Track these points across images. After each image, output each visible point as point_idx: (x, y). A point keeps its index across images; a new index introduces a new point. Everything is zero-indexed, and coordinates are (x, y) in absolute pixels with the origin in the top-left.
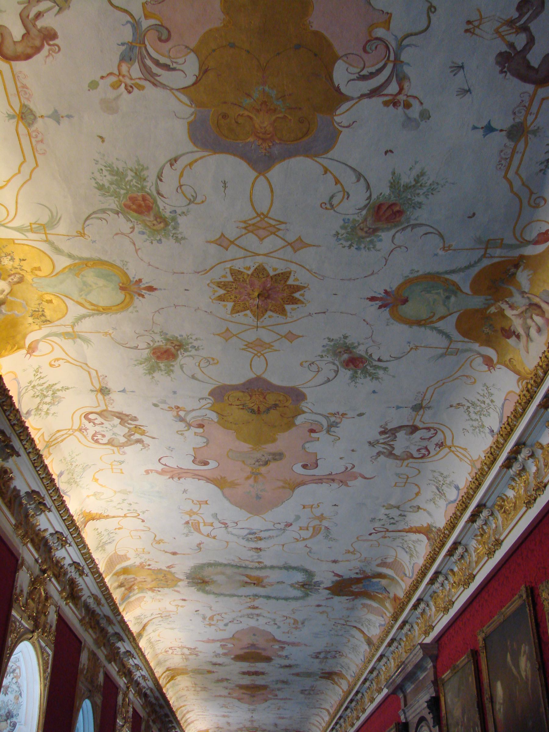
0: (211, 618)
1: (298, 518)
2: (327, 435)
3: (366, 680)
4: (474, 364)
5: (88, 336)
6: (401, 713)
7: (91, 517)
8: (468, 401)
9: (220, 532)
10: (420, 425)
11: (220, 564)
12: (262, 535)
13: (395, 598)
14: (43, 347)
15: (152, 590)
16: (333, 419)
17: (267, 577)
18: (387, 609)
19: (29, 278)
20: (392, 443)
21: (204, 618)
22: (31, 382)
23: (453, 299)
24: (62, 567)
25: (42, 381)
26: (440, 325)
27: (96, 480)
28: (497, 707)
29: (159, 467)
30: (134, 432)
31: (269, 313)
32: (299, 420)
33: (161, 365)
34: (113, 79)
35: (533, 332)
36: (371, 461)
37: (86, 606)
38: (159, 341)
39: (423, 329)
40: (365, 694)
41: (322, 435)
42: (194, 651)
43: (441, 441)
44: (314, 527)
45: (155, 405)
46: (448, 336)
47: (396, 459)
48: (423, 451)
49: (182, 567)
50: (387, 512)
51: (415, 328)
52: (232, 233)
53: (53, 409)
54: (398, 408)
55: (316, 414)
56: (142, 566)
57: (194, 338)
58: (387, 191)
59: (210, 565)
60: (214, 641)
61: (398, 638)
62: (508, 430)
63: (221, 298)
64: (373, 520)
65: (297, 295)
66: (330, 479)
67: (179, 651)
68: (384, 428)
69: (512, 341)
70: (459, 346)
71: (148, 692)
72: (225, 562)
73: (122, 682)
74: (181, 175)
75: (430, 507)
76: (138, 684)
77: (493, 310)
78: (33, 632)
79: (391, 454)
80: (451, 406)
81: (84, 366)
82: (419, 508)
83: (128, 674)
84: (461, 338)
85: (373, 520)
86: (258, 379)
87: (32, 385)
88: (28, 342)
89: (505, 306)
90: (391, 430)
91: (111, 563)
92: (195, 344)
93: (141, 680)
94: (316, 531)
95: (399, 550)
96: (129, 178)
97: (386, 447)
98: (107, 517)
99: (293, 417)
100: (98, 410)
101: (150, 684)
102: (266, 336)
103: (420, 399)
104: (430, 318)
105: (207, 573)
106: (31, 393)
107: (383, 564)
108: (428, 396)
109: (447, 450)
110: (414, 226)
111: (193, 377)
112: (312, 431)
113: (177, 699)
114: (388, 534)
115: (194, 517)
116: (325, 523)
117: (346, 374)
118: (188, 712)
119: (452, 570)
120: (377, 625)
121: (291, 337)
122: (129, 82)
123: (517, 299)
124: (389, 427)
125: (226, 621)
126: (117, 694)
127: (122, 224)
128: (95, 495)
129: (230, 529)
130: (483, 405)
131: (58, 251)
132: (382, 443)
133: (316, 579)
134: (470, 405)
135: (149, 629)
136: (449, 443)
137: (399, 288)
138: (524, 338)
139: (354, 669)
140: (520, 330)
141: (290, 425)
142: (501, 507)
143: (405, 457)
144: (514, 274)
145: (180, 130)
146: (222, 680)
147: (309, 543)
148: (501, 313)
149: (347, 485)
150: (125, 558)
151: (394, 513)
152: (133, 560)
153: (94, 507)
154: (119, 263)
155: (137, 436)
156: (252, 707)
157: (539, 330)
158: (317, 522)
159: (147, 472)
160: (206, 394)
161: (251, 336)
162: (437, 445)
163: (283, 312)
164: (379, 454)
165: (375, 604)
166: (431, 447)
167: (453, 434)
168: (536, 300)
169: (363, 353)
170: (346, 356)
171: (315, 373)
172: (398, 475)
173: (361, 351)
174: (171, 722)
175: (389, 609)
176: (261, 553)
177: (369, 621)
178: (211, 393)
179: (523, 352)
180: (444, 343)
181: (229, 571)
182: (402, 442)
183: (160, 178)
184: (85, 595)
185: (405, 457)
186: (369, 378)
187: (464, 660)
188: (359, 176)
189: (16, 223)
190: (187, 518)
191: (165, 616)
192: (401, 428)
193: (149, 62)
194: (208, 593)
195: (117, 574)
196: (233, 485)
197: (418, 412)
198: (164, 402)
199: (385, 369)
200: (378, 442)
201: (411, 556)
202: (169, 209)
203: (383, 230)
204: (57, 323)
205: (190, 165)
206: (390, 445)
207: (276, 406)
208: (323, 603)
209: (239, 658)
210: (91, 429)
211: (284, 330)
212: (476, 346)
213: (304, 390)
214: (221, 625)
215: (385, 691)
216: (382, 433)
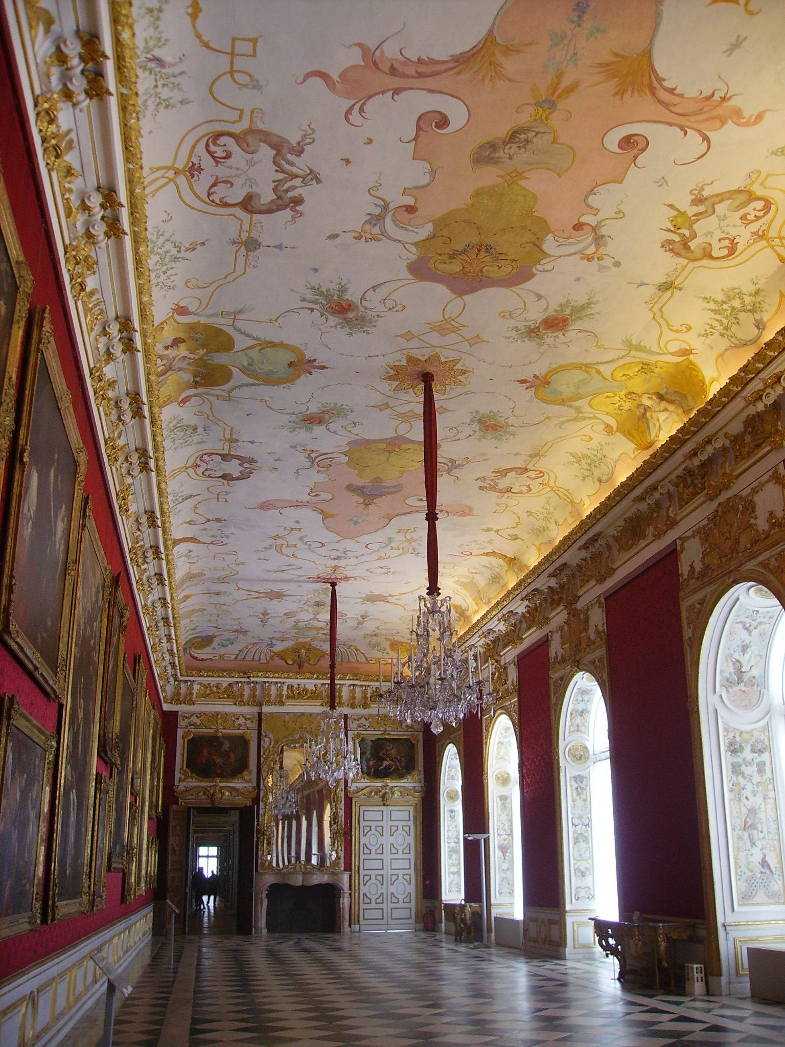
2: (389, 200)
4: (197, 303)
8: (183, 258)
10: (238, 211)
14: (674, 347)
16: (376, 230)
20: (281, 176)
22: (722, 335)
23: (246, 364)
25: (715, 323)
31: (423, 359)
32: (426, 231)
36: (313, 130)
39: (267, 339)
43: (196, 178)
45: (617, 264)
47: (266, 133)
51: (277, 341)
54: (280, 247)
55: (399, 241)
57: (511, 339)
63: (463, 372)
65: (393, 373)
68: (298, 212)
70: (223, 321)
80: (203, 244)
84: (224, 328)
86: (461, 294)
87: (725, 331)
89: (192, 356)
90: (285, 207)
97: (288, 167)
99: (434, 237)
102: (435, 339)
103: (250, 258)
104: (263, 349)
106: (734, 328)
109: (180, 165)
112: (411, 209)
117: (353, 295)
121: (409, 336)
123: (184, 365)
124: (287, 214)
130: (164, 269)
132: (297, 176)
134: (180, 255)
136: (182, 180)
137: (299, 376)
141: (441, 224)
143: (250, 139)
144: (195, 376)
161: (452, 338)
162: (200, 170)
166: (207, 162)
167: (181, 197)
170: (351, 315)
171: (391, 297)
173: (333, 320)
180: (239, 324)
185: (250, 139)
186: (323, 289)
197: (248, 238)
199: (304, 300)
200: (305, 183)
204: (638, 360)
206: (283, 172)
207: (452, 256)
211: (414, 343)
212: (203, 320)
213: (409, 276)
216: (298, 201)
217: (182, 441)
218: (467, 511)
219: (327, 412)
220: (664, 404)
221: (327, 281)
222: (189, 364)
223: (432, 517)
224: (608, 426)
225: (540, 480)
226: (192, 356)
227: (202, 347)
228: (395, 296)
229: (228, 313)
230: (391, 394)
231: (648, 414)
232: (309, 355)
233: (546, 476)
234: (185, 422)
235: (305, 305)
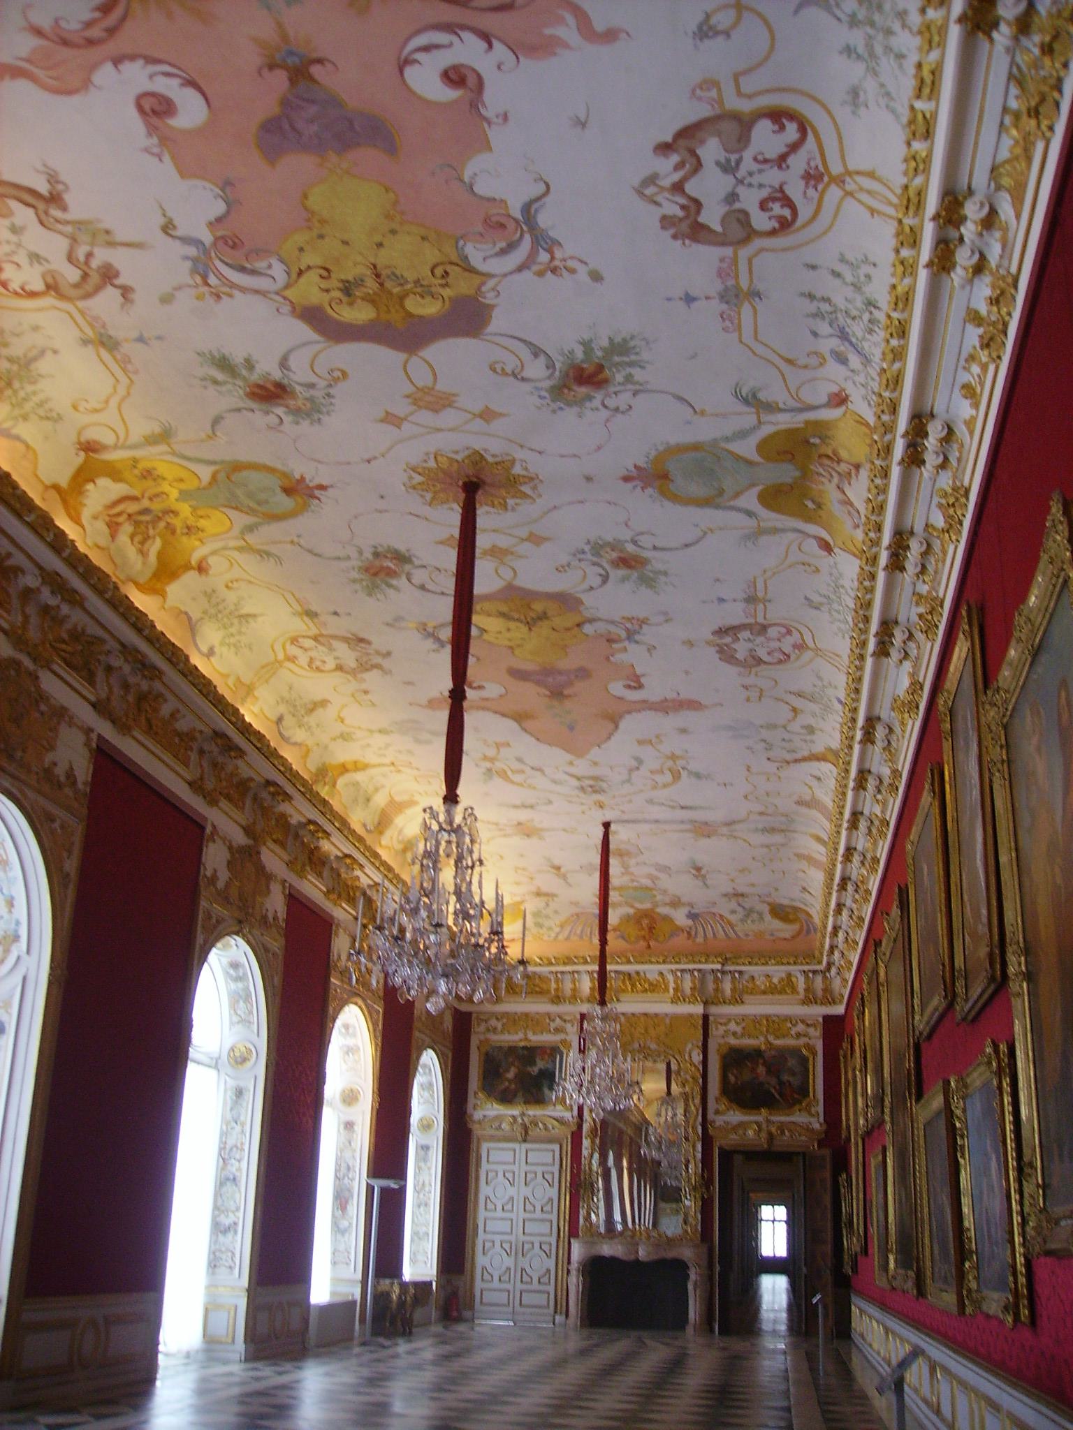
156: (582, 767)
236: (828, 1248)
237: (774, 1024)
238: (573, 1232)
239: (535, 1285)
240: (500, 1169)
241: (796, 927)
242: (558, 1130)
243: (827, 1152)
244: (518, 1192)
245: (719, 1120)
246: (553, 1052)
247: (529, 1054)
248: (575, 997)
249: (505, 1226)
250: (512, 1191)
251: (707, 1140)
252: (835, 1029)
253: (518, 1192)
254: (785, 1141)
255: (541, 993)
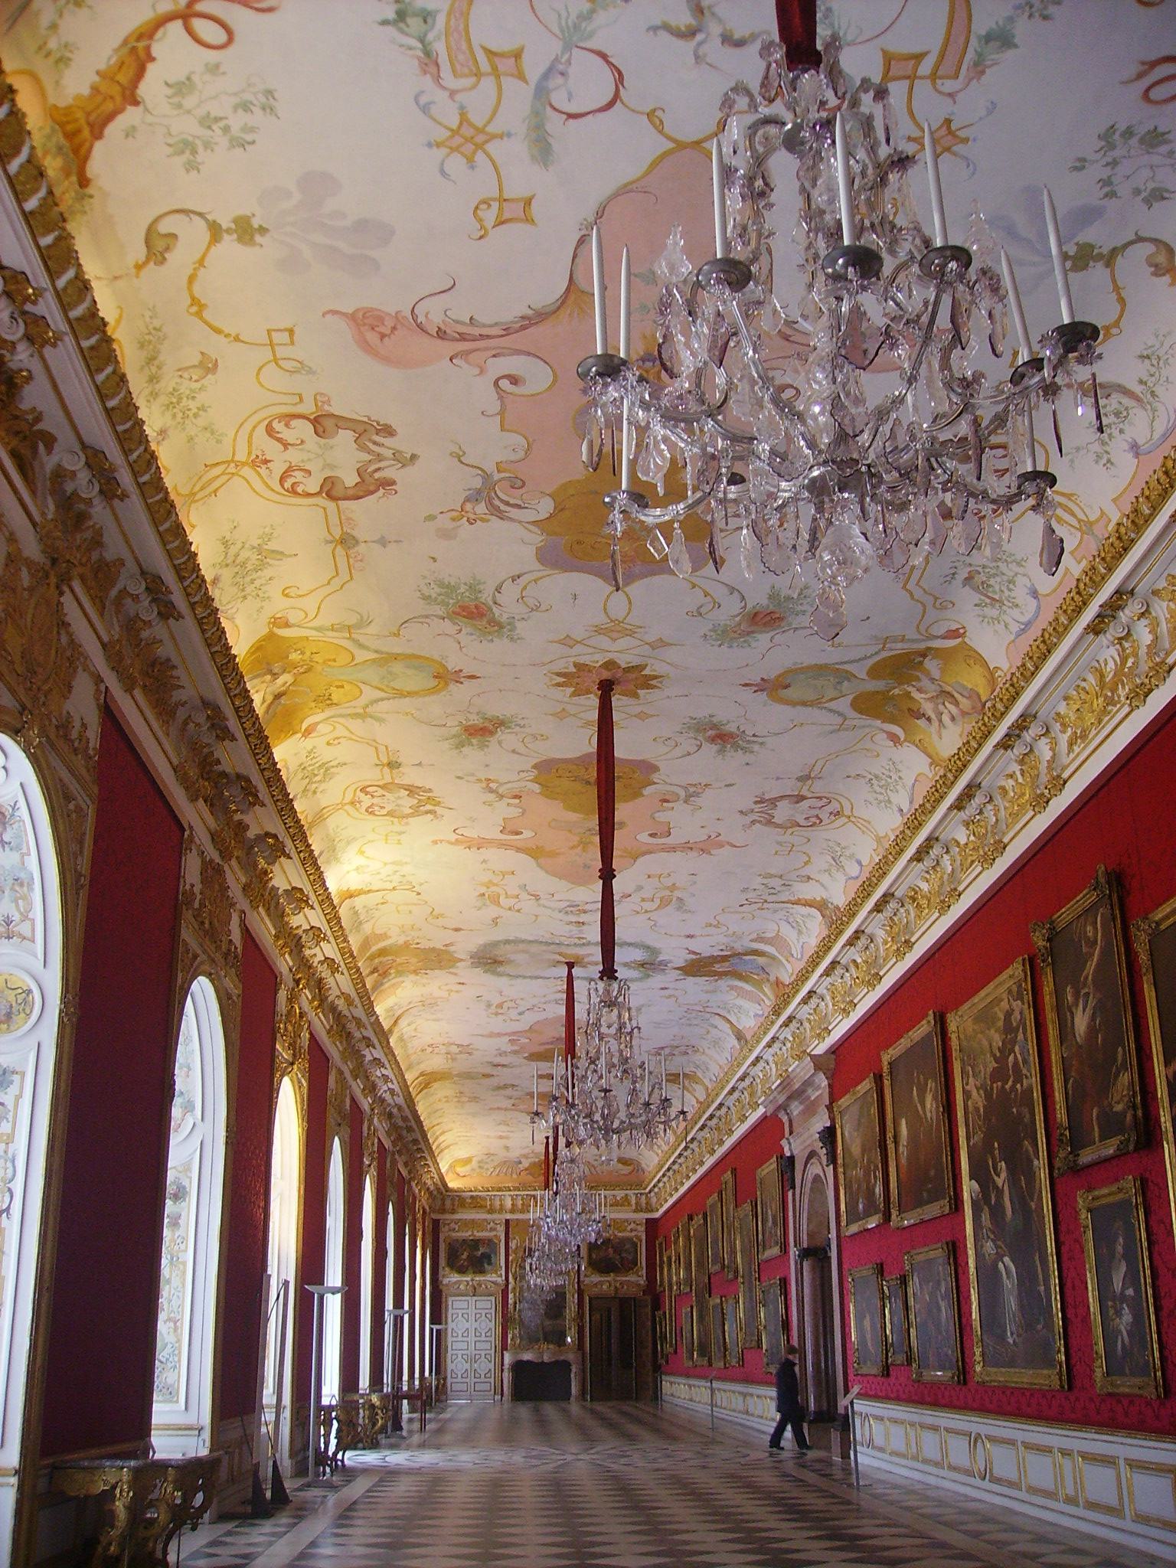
0: (500, 1006)
1: (640, 888)
3: (733, 1089)
5: (385, 716)
6: (784, 1142)
7: (350, 895)
9: (528, 905)
11: (523, 941)
12: (587, 907)
13: (778, 983)
15: (416, 972)
16: (692, 790)
17: (589, 955)
18: (765, 995)
19: (319, 668)
21: (489, 1006)
24: (310, 967)
26: (832, 705)
27: (362, 853)
28: (901, 1149)
29: (453, 837)
30: (424, 802)
32: (648, 791)
33: (474, 741)
34: (454, 514)
35: (946, 718)
37: (333, 1009)
38: (475, 720)
40: (732, 1108)
41: (679, 806)
42: (466, 1050)
44: (661, 899)
46: (840, 714)
48: (814, 820)
49: (465, 945)
50: (765, 881)
51: (799, 708)
52: (579, 634)
53: (323, 786)
56: (407, 944)
58: (765, 602)
59: (507, 942)
60: (499, 1035)
61: (781, 1037)
62: (914, 823)
64: (745, 890)
66: (687, 847)
67: (443, 1049)
69: (922, 722)
70: (855, 722)
71: (395, 1111)
72: (531, 938)
73: (365, 1103)
74: (525, 588)
75: (825, 878)
76: (382, 1100)
77: (896, 691)
78: (292, 1064)
79: (769, 822)
81: (374, 744)
82: (809, 878)
83: (371, 1088)
85: (745, 890)
88: (304, 726)
89: (910, 689)
91: (366, 944)
92: (522, 723)
93: (387, 1096)
94: (665, 903)
95: (783, 924)
96: (462, 590)
98: (369, 891)
100: (380, 783)
101: (400, 1100)
105: (500, 952)
107: (760, 939)
108: (817, 768)
110: (796, 629)
111: (514, 751)
113: (429, 1115)
114: (766, 905)
115: (494, 889)
116: (677, 894)
118: (443, 1133)
119: (854, 961)
120: (752, 1014)
121: (642, 716)
122: (472, 516)
123: (925, 683)
125: (521, 1009)
126: (362, 1123)
127: (448, 627)
128: (357, 869)
129: (541, 902)
131: (361, 646)
133: (661, 958)
135: (403, 1023)
136: (847, 812)
138: (935, 723)
139: (714, 1069)
140: (931, 713)
142: (914, 899)
144: (921, 663)
145: (529, 553)
146: (505, 1087)
147: (654, 916)
148: (908, 695)
149: (709, 853)
150: (384, 936)
151: (776, 883)
152: (396, 939)
153: (354, 882)
154: (436, 657)
155: (429, 807)
157: (953, 719)
158: (668, 893)
159: (435, 842)
160: (528, 766)
163: (636, 696)
164: (753, 822)
165: (748, 987)
166: (824, 816)
168: (949, 689)
169: (734, 730)
172: (780, 843)
173: (732, 728)
174: (419, 1150)
175: (769, 998)
176: (584, 927)
177: (740, 1007)
178: (535, 767)
179: (935, 737)
180: (840, 720)
181: (534, 948)
182: (783, 812)
183: (498, 590)
184: (333, 993)
187: (866, 1085)
188: (732, 590)
189: (316, 623)
190: (483, 890)
191: (428, 1004)
192: (782, 797)
193: (497, 502)
194: (500, 975)
195: (372, 958)
196: (553, 854)
198: (473, 775)
201: (800, 932)
202: (505, 616)
203: (761, 632)
205: (535, 581)
208: (671, 986)
209: (535, 1057)
210: (367, 801)
214: (513, 1014)
215: (761, 1110)
216: (756, 803)
217: (1003, 567)
218: (372, 337)
219: (741, 635)
220: (269, 699)
221: (735, 759)
222: (918, 679)
223: (607, 875)
224: (287, 625)
225: (278, 468)
226: (910, 689)
227: (893, 697)
228: (667, 749)
229: (847, 730)
230: (650, 661)
231: (268, 677)
232: (763, 696)
233: (278, 488)
234: (976, 598)
235: (760, 740)
236: (649, 1351)
237: (617, 1224)
238: (504, 1347)
239: (483, 1379)
240: (460, 1312)
241: (630, 1168)
242: (493, 1288)
243: (648, 1298)
244: (472, 1325)
245: (587, 1281)
246: (489, 1242)
247: (476, 1243)
248: (502, 1209)
249: (464, 1346)
250: (467, 1325)
251: (580, 1293)
252: (652, 1225)
253: (472, 1325)
254: (625, 1292)
255: (481, 1207)
